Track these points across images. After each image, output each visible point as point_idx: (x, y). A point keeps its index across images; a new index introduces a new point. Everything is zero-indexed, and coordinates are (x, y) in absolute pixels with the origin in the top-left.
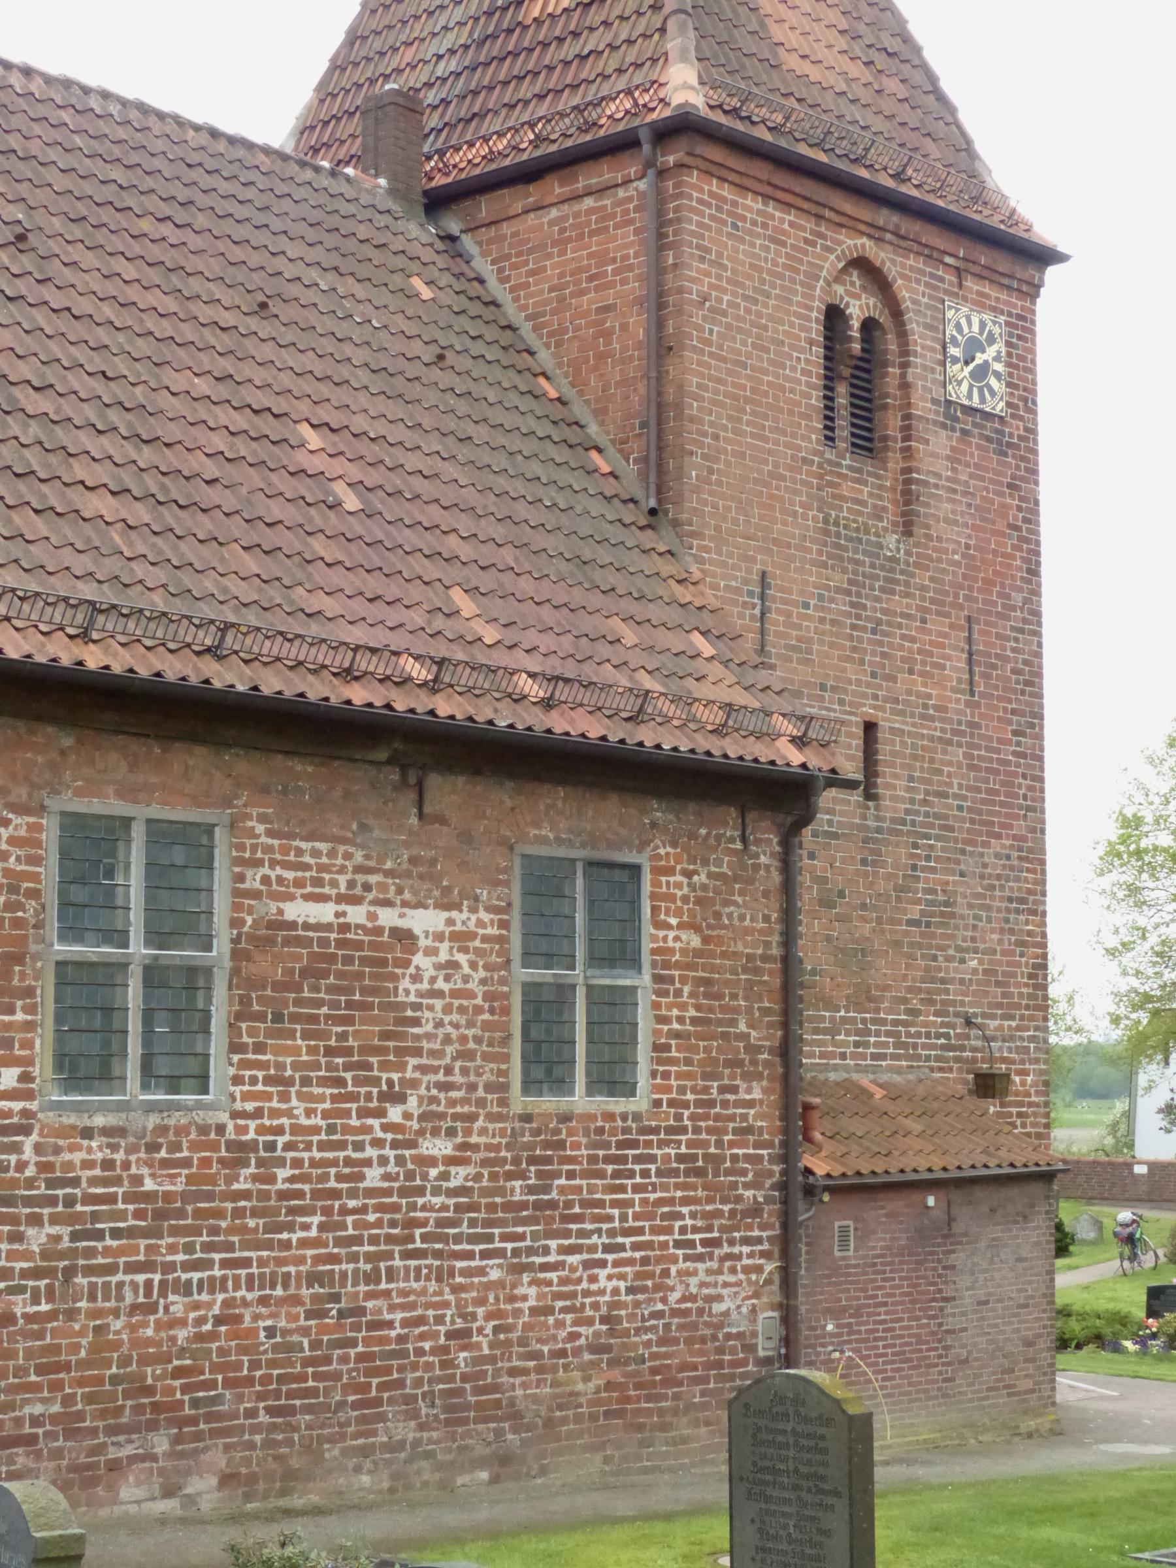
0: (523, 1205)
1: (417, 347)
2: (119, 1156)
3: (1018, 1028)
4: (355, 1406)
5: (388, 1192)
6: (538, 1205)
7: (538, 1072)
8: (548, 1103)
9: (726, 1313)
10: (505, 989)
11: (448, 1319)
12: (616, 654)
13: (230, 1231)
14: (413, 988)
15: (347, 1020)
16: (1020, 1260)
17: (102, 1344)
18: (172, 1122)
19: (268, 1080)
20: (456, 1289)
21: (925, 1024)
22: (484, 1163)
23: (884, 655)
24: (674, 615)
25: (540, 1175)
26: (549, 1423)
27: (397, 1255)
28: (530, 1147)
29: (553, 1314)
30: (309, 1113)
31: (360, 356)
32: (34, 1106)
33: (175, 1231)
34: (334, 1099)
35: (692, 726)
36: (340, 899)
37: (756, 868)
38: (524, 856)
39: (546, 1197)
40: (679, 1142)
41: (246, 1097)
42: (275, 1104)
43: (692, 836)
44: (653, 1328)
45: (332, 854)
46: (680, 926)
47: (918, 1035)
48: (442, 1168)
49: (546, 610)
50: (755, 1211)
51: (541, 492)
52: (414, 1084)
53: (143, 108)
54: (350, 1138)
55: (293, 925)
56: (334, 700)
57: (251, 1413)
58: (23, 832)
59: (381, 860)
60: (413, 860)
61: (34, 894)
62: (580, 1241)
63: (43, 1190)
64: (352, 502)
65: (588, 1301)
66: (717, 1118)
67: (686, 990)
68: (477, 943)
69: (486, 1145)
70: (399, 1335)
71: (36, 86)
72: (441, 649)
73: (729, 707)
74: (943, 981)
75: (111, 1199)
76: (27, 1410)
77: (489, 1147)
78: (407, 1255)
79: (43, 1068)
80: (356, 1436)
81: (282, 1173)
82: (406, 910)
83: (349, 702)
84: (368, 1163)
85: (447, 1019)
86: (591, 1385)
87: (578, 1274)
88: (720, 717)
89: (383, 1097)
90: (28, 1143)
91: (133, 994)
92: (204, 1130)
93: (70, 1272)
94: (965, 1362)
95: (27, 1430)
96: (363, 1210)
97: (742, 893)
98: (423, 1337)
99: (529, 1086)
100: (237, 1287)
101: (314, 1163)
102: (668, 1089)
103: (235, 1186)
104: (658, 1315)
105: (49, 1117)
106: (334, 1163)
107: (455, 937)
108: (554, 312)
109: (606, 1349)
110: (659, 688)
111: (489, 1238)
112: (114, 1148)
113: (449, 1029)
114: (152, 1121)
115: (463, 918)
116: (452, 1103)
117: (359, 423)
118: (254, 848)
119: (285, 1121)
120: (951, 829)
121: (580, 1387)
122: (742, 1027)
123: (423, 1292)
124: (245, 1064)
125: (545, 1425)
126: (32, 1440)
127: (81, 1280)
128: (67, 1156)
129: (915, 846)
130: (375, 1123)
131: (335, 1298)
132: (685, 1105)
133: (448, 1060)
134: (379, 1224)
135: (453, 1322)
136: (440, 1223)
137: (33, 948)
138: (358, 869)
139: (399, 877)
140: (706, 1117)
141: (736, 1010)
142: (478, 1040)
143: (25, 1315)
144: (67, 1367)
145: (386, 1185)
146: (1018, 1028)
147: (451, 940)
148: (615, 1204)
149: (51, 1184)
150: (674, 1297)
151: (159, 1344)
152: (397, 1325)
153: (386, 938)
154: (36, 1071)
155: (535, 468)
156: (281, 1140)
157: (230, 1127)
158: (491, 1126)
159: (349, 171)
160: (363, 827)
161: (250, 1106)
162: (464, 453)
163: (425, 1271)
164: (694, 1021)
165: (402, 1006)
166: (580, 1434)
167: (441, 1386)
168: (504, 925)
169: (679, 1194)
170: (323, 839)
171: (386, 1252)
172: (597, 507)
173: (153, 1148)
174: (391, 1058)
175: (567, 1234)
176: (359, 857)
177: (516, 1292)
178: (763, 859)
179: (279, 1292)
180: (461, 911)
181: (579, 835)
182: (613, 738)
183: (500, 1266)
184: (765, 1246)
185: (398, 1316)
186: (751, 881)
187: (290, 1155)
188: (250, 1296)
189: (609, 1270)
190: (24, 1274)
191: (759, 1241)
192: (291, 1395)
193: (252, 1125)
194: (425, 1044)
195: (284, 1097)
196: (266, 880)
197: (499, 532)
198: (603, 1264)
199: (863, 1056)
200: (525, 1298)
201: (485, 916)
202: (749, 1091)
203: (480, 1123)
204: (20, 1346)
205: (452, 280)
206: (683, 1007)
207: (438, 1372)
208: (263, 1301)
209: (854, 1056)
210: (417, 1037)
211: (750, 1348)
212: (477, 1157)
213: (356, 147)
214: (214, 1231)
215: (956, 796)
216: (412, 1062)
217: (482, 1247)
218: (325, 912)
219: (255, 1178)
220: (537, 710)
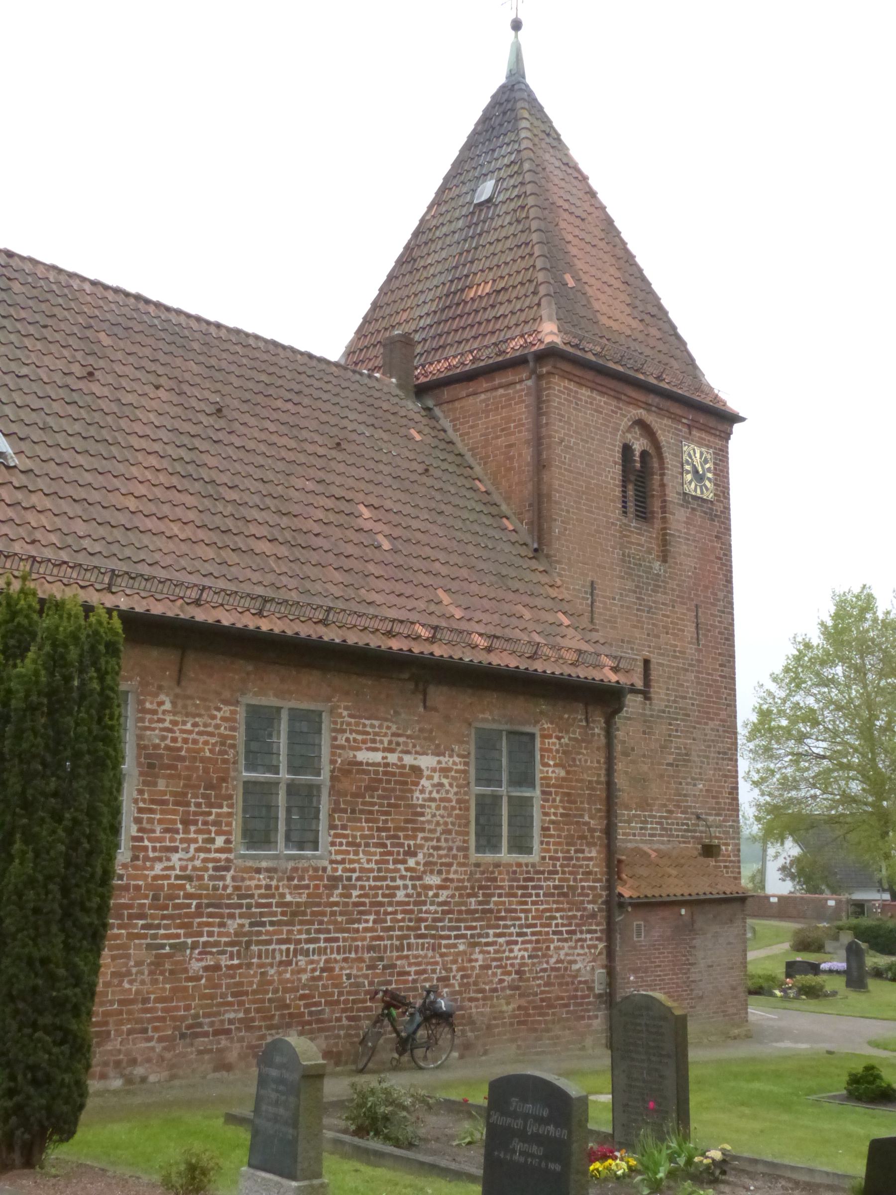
0: (476, 911)
1: (414, 465)
2: (274, 883)
3: (724, 821)
5: (408, 904)
6: (484, 911)
7: (483, 842)
8: (488, 857)
9: (579, 970)
12: (522, 624)
13: (329, 923)
14: (421, 797)
15: (387, 813)
16: (729, 943)
17: (265, 982)
18: (300, 865)
19: (349, 844)
20: (442, 955)
21: (676, 818)
22: (457, 889)
23: (653, 624)
24: (549, 604)
25: (484, 895)
26: (489, 1027)
28: (479, 880)
30: (369, 861)
31: (387, 470)
32: (231, 856)
33: (302, 923)
34: (381, 854)
35: (561, 661)
36: (385, 750)
37: (593, 735)
38: (476, 728)
41: (338, 852)
42: (351, 856)
43: (561, 718)
44: (541, 978)
45: (380, 727)
46: (555, 765)
47: (673, 824)
49: (485, 601)
50: (593, 915)
51: (479, 540)
52: (421, 847)
53: (275, 344)
55: (361, 763)
56: (383, 648)
57: (339, 1019)
58: (228, 714)
59: (405, 729)
60: (421, 730)
61: (233, 746)
63: (235, 900)
64: (386, 545)
66: (574, 866)
67: (558, 799)
68: (453, 773)
71: (223, 334)
72: (434, 621)
73: (580, 652)
74: (685, 795)
75: (269, 905)
76: (227, 1016)
77: (459, 880)
79: (237, 836)
81: (355, 893)
83: (390, 648)
84: (398, 888)
85: (438, 813)
86: (511, 1007)
88: (575, 657)
90: (229, 875)
91: (282, 799)
92: (316, 869)
93: (249, 944)
94: (701, 998)
95: (226, 1026)
96: (395, 913)
97: (586, 748)
98: (425, 980)
99: (478, 849)
100: (332, 952)
101: (371, 888)
102: (548, 851)
103: (332, 899)
104: (545, 970)
105: (239, 862)
106: (381, 888)
108: (484, 447)
109: (517, 988)
110: (543, 641)
111: (458, 928)
112: (271, 878)
113: (439, 818)
114: (291, 865)
115: (446, 760)
116: (440, 857)
117: (388, 504)
118: (342, 723)
119: (356, 866)
120: (688, 716)
121: (505, 1008)
122: (587, 818)
123: (426, 956)
124: (337, 836)
126: (227, 1032)
127: (254, 948)
128: (248, 883)
129: (670, 724)
130: (401, 867)
131: (381, 959)
132: (558, 859)
134: (403, 920)
136: (435, 920)
137: (232, 774)
138: (393, 735)
140: (568, 866)
141: (583, 809)
142: (453, 824)
143: (226, 966)
144: (246, 993)
146: (724, 821)
148: (522, 911)
149: (240, 897)
150: (552, 960)
151: (293, 982)
154: (233, 838)
155: (476, 528)
156: (355, 875)
157: (329, 868)
158: (459, 869)
159: (377, 375)
160: (397, 713)
161: (339, 858)
162: (440, 519)
164: (562, 815)
165: (415, 806)
168: (466, 764)
170: (377, 719)
172: (507, 548)
173: (290, 879)
175: (498, 927)
176: (394, 728)
178: (597, 731)
179: (353, 955)
182: (522, 667)
184: (599, 935)
185: (413, 969)
186: (590, 742)
187: (359, 883)
188: (338, 957)
189: (519, 946)
190: (227, 944)
191: (595, 931)
192: (359, 1010)
193: (340, 867)
194: (427, 826)
195: (356, 853)
196: (347, 740)
197: (460, 560)
198: (516, 943)
199: (644, 835)
200: (477, 960)
201: (457, 759)
202: (590, 852)
203: (454, 868)
204: (224, 982)
205: (430, 431)
206: (556, 807)
208: (345, 960)
209: (640, 835)
210: (423, 822)
211: (591, 989)
213: (379, 362)
214: (321, 923)
215: (691, 698)
216: (420, 835)
218: (377, 757)
219: (342, 895)
220: (484, 653)
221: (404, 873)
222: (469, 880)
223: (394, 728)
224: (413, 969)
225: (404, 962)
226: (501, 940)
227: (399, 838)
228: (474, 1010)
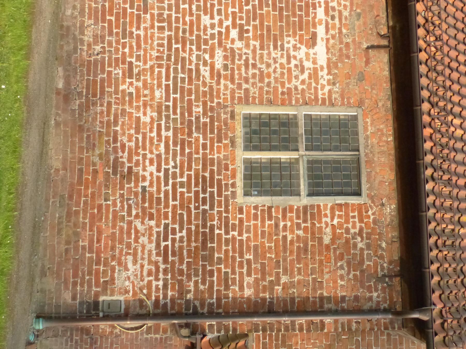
0: (190, 114)
4: (103, 6)
5: (199, 29)
10: (294, 102)
11: (138, 63)
14: (290, 45)
22: (211, 88)
25: (205, 124)
26: (81, 128)
27: (170, 33)
29: (136, 133)
39: (194, 129)
40: (220, 229)
48: (209, 61)
52: (247, 46)
54: (223, 8)
60: (347, 45)
62: (171, 152)
65: (140, 158)
66: (234, 258)
68: (314, 85)
69: (220, 89)
70: (133, 33)
77: (218, 91)
78: (169, 38)
80: (90, 6)
82: (325, 40)
84: (212, 18)
85: (278, 65)
86: (97, 159)
87: (155, 151)
89: (241, 26)
96: (191, 15)
98: (131, 47)
99: (248, 118)
107: (315, 70)
116: (239, 69)
121: (97, 152)
122: (284, 279)
123: (152, 49)
125: (80, 126)
130: (229, 23)
132: (240, 234)
133: (259, 66)
134: (185, 23)
135: (137, 66)
138: (340, 12)
139: (339, 37)
141: (292, 276)
145: (202, 27)
147: (314, 68)
150: (138, 223)
152: (138, 32)
153: (312, 30)
158: (228, 92)
160: (359, 15)
163: (161, 49)
164: (285, 237)
165: (282, 36)
166: (73, 152)
167: (107, 59)
169: (193, 228)
171: (171, 27)
174: (259, 32)
175: (175, 144)
176: (346, 13)
177: (148, 108)
180: (327, 75)
181: (371, 152)
183: (161, 98)
185: (142, 33)
194: (265, 52)
200: (145, 114)
201: (327, 88)
203: (230, 86)
207: (114, 56)
210: (268, 48)
211: (105, 291)
212: (214, 84)
216: (257, 44)
217: (171, 86)
221: (225, 25)
222: (219, 103)
223: (346, 13)
224: (142, 33)
225: (148, 24)
226: (162, 148)
227: (254, 20)
228: (99, 109)
